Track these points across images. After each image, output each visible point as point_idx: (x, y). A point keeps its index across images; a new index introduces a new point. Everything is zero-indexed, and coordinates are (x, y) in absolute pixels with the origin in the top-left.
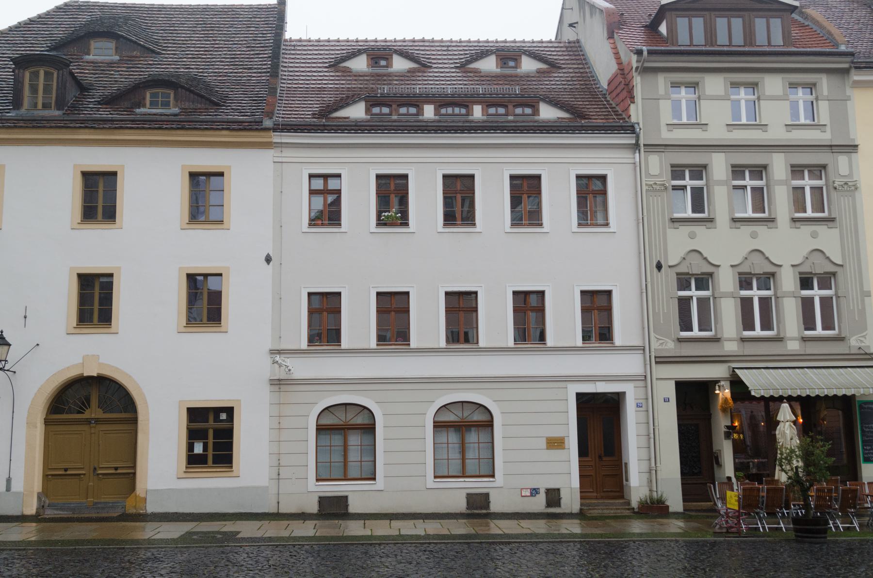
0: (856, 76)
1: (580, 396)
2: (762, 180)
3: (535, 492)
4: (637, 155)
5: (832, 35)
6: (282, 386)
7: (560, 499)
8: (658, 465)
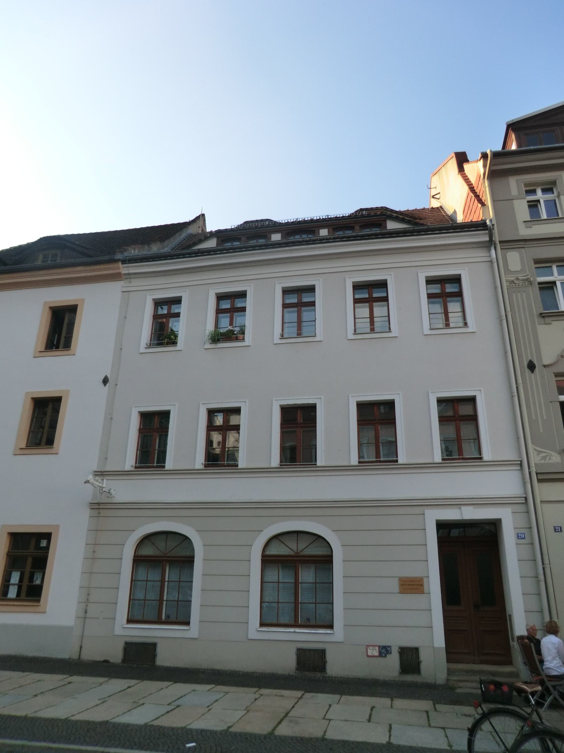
3: (385, 651)
4: (493, 252)
6: (101, 511)
7: (419, 663)
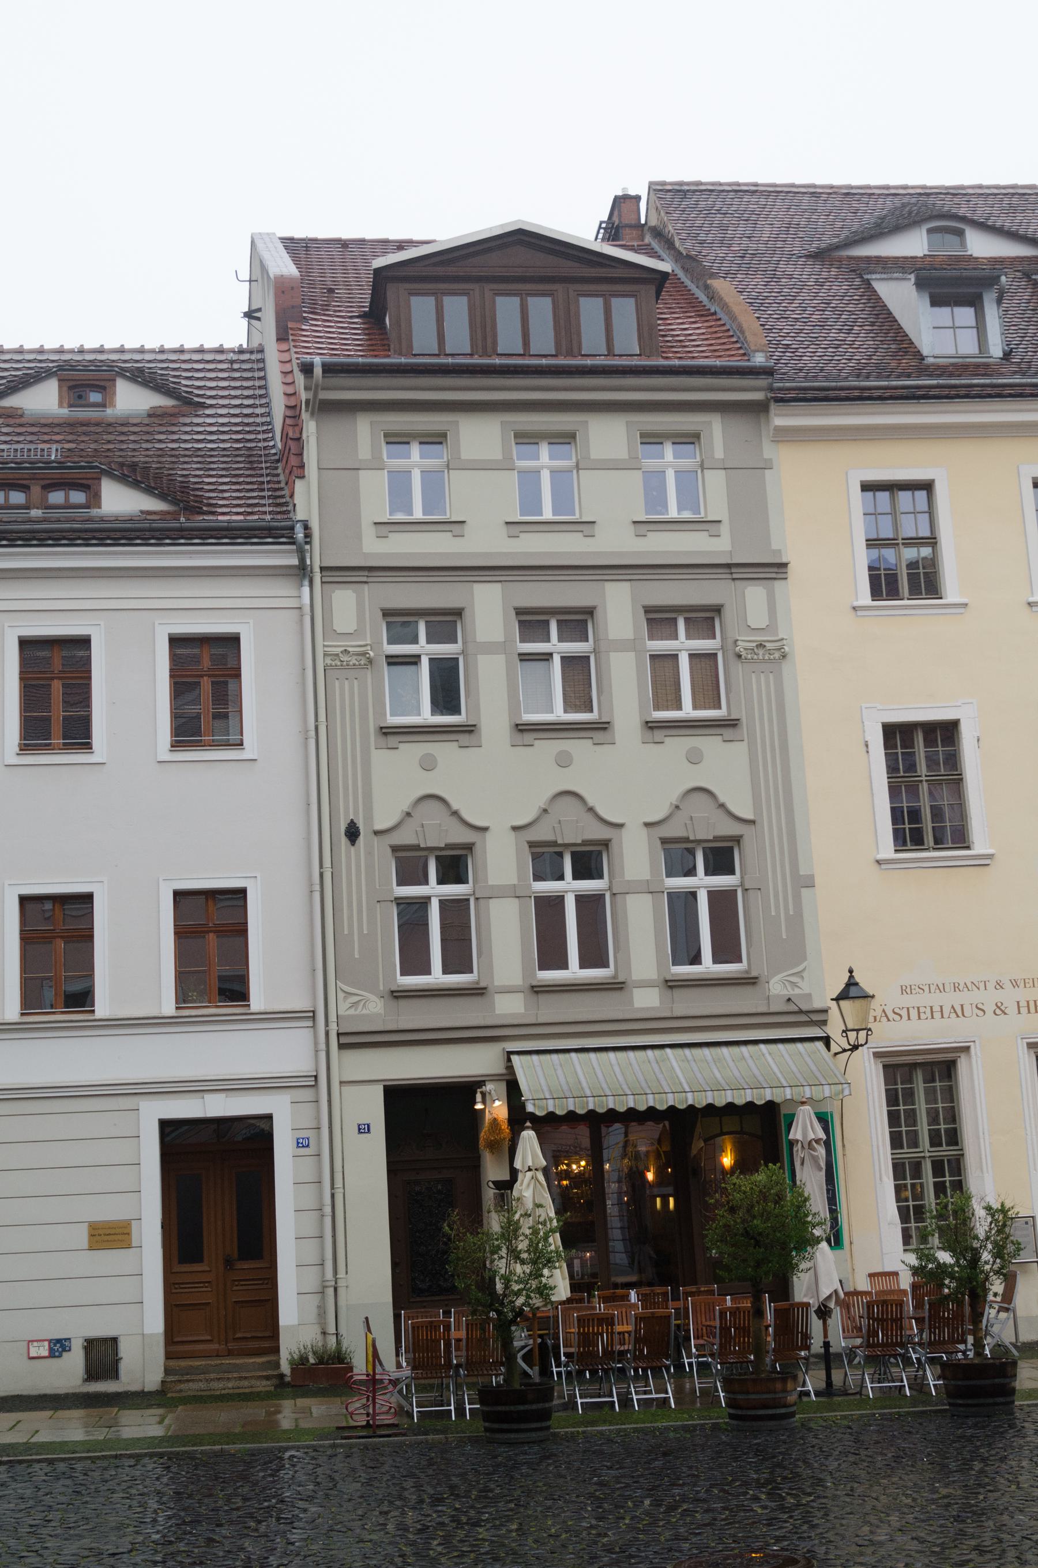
0: (781, 419)
1: (167, 1127)
2: (714, 638)
3: (59, 1347)
4: (306, 590)
5: (742, 332)
7: (117, 1361)
8: (341, 1274)
